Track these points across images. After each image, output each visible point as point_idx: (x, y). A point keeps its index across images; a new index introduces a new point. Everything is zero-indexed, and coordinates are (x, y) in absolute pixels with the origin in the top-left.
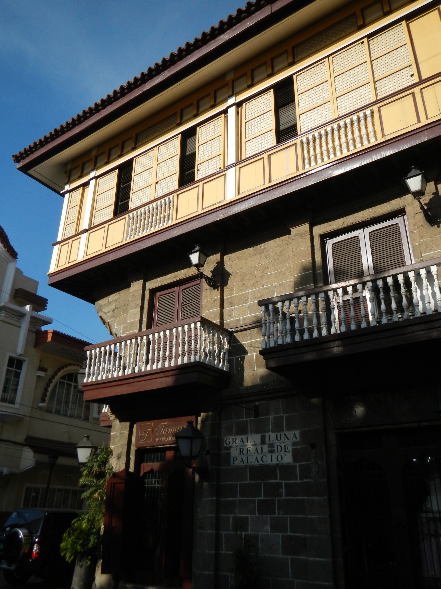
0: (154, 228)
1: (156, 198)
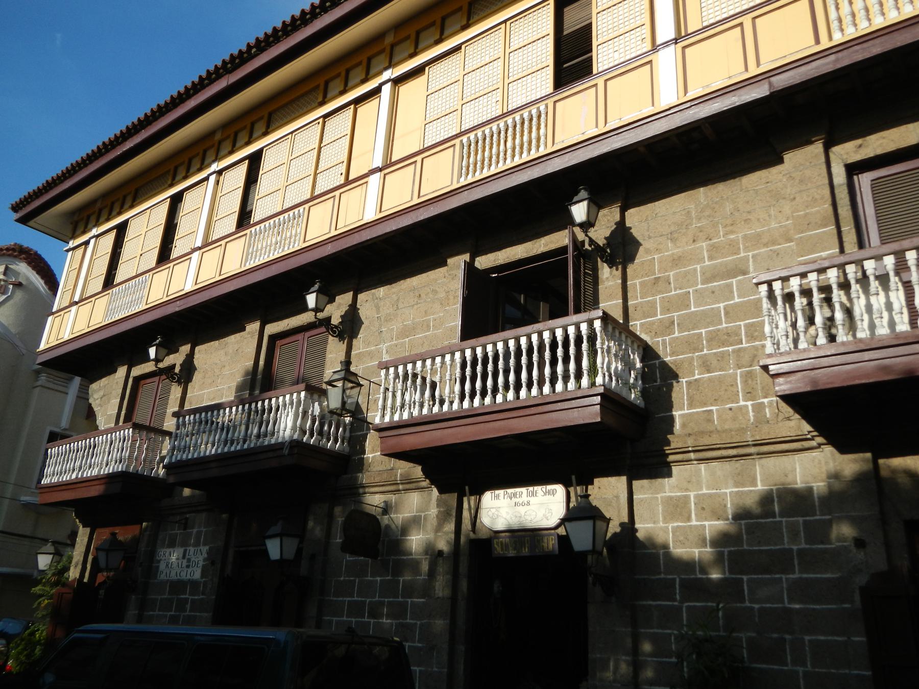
0: (268, 256)
1: (284, 208)
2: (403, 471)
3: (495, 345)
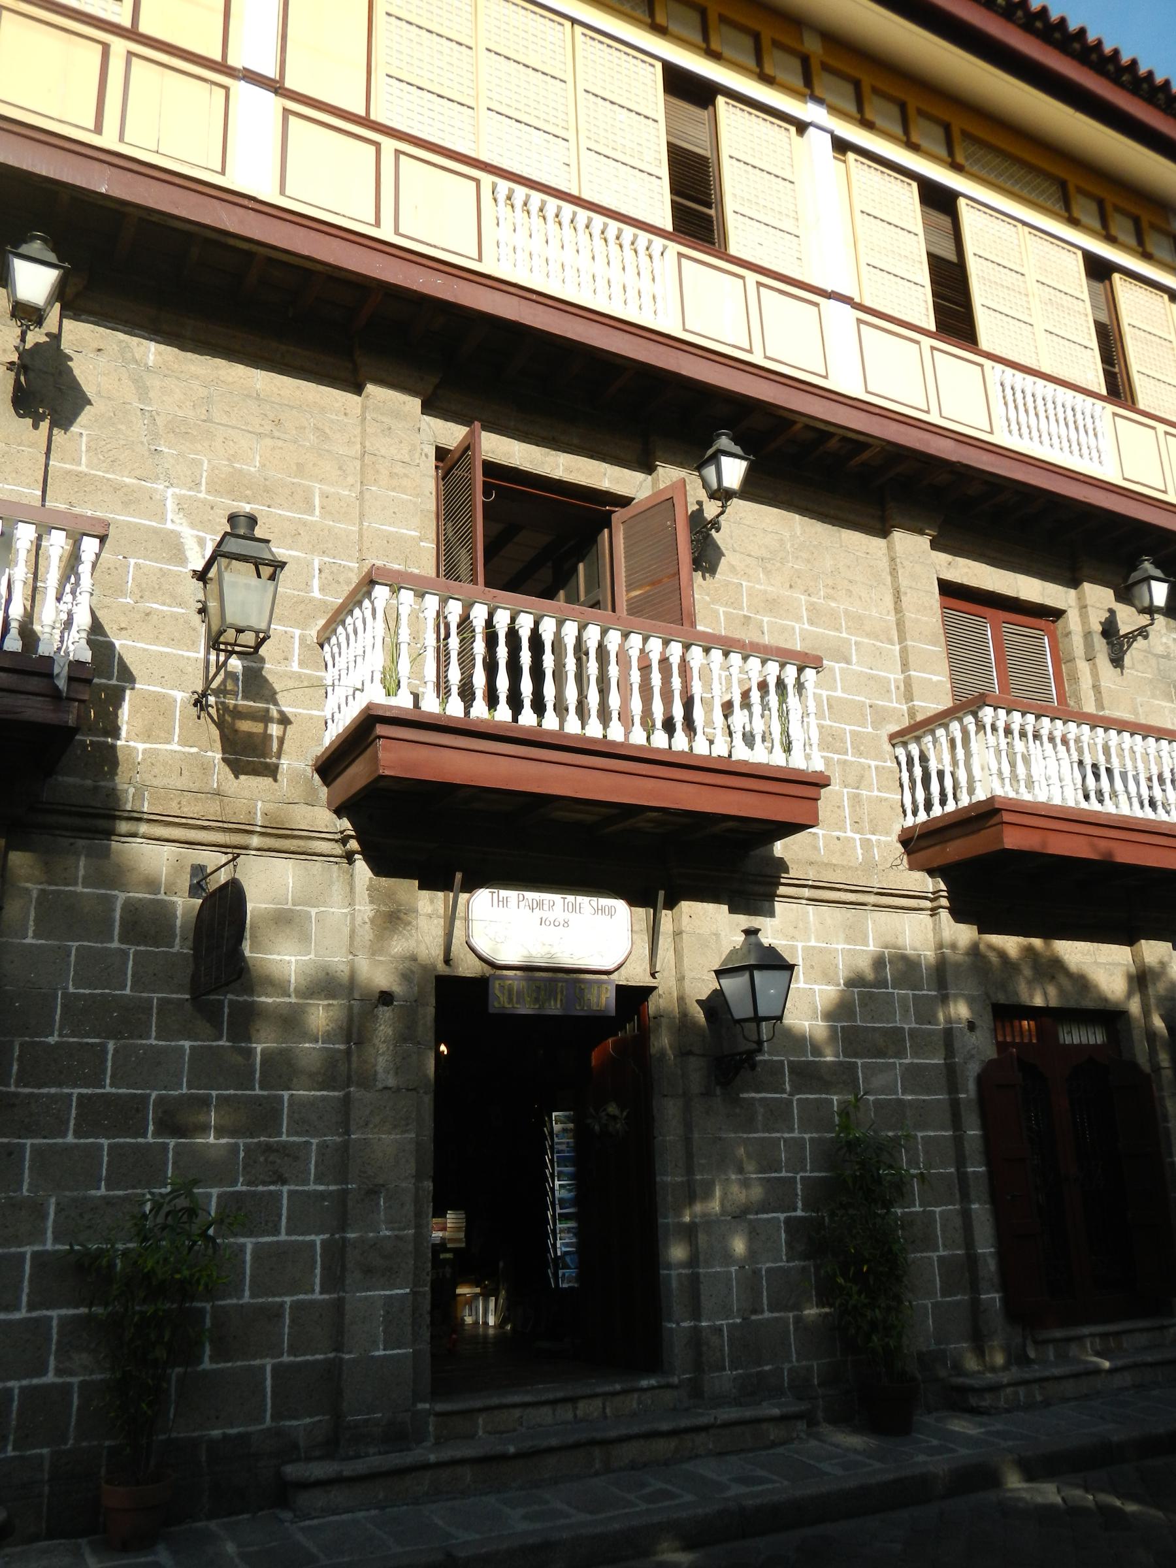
2: (271, 807)
3: (468, 607)
